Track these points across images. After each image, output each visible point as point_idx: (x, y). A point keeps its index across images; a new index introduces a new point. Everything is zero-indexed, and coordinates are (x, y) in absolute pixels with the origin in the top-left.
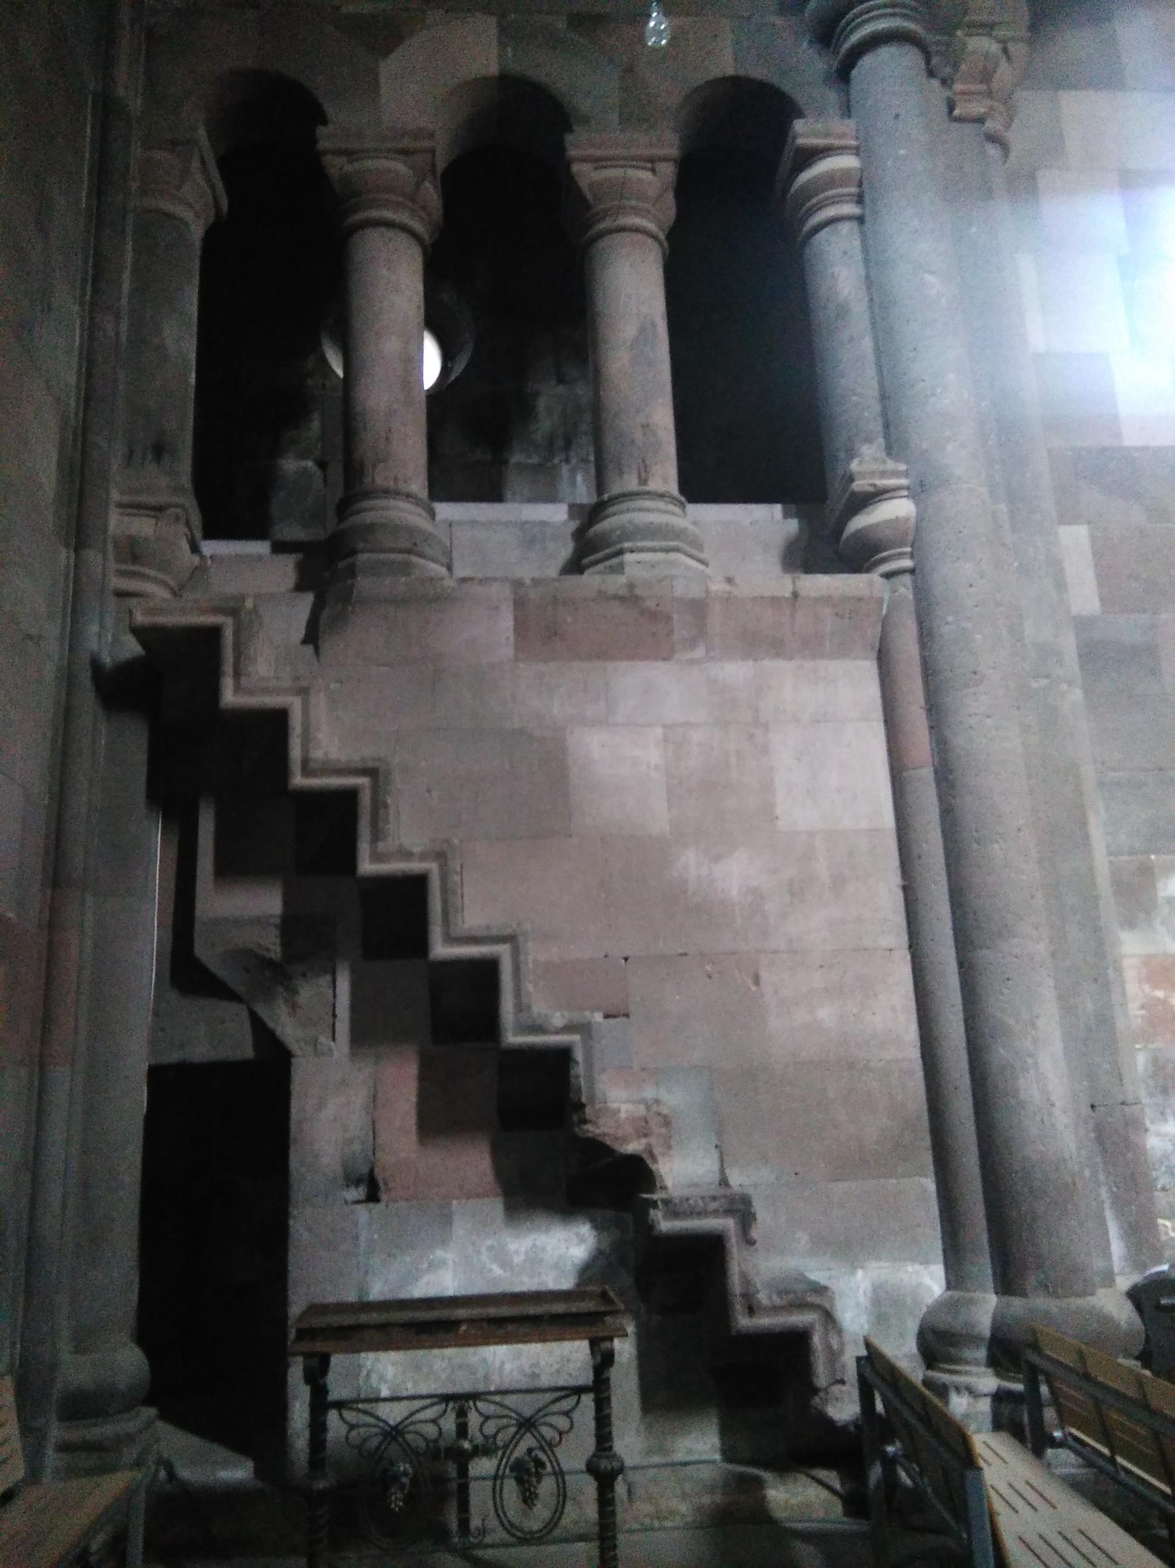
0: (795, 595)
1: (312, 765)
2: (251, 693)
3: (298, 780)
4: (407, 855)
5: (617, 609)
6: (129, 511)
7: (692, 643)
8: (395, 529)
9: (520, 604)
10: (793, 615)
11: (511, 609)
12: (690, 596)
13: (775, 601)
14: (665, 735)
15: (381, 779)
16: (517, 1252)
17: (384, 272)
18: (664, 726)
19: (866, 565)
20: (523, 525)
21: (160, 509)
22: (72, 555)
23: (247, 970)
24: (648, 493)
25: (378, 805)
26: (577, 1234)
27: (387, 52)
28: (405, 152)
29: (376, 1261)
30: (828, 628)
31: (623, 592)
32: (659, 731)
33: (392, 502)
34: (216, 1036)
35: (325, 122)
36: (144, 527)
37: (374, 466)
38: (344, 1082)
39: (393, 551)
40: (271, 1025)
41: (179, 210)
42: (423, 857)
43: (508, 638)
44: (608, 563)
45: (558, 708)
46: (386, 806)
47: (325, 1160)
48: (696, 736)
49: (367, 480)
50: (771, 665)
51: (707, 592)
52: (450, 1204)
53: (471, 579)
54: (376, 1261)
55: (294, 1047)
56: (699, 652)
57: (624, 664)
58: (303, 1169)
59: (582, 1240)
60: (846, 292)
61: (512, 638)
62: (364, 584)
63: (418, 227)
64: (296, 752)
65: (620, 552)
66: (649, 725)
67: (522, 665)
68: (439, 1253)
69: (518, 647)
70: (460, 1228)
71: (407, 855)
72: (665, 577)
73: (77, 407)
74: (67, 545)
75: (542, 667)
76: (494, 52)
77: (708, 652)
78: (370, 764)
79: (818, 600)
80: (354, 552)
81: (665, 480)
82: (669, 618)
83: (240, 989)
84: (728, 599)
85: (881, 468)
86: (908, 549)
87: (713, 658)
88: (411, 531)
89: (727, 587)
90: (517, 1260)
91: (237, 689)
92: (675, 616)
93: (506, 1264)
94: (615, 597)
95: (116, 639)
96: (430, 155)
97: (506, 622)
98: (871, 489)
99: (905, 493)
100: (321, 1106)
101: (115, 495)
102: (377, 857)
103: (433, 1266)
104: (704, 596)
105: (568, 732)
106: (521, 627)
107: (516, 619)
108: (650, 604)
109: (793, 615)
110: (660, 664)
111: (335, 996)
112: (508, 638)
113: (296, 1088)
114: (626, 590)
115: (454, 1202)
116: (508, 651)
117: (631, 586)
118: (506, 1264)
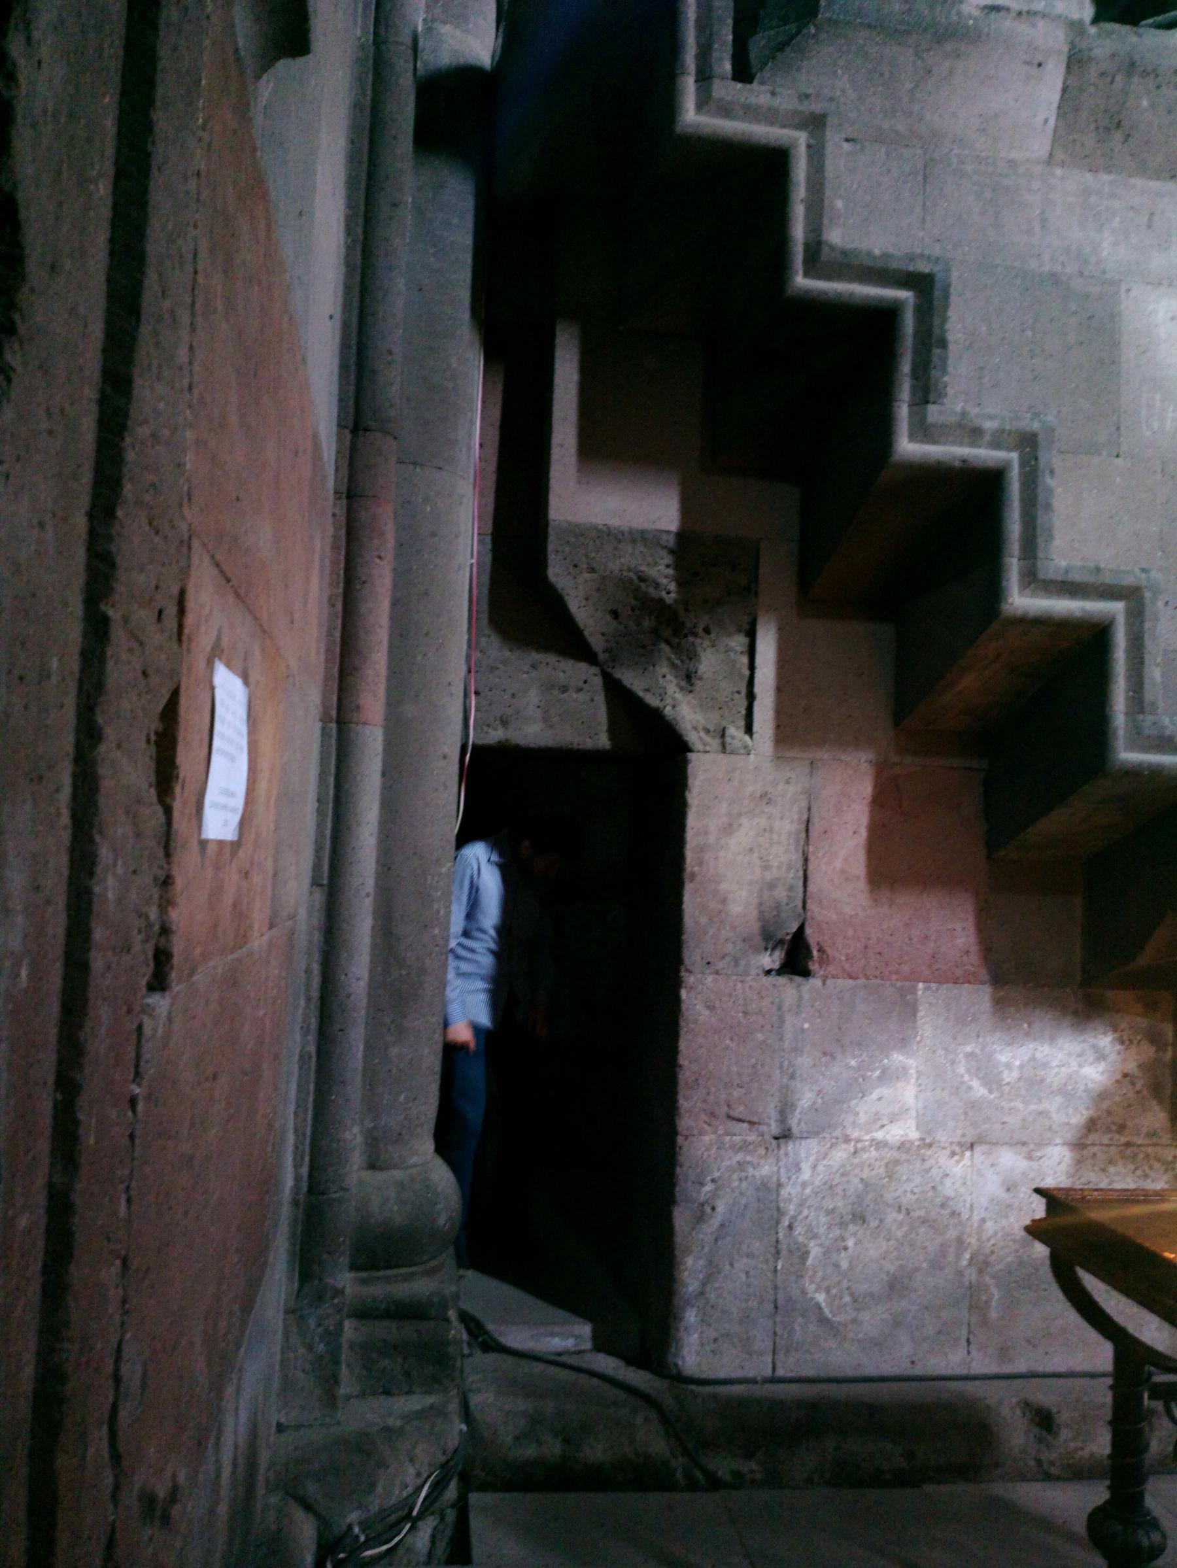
3: (801, 281)
4: (975, 434)
11: (1062, 69)
15: (937, 293)
16: (1008, 1066)
23: (615, 614)
25: (931, 341)
26: (1094, 1046)
29: (804, 1062)
34: (553, 708)
38: (765, 798)
40: (652, 700)
42: (995, 444)
43: (1046, 121)
45: (1111, 250)
46: (943, 344)
47: (735, 909)
52: (914, 991)
53: (1008, 9)
54: (804, 1062)
55: (693, 738)
58: (703, 920)
59: (1101, 1057)
64: (798, 231)
67: (1059, 172)
68: (898, 1057)
69: (1055, 140)
70: (927, 1026)
71: (975, 434)
78: (924, 267)
83: (596, 642)
90: (1009, 1077)
91: (700, 106)
93: (992, 1081)
100: (728, 829)
102: (923, 431)
103: (888, 1077)
105: (1123, 288)
107: (1065, 89)
111: (752, 667)
112: (1046, 121)
113: (694, 797)
115: (921, 985)
116: (1040, 146)
118: (992, 1081)
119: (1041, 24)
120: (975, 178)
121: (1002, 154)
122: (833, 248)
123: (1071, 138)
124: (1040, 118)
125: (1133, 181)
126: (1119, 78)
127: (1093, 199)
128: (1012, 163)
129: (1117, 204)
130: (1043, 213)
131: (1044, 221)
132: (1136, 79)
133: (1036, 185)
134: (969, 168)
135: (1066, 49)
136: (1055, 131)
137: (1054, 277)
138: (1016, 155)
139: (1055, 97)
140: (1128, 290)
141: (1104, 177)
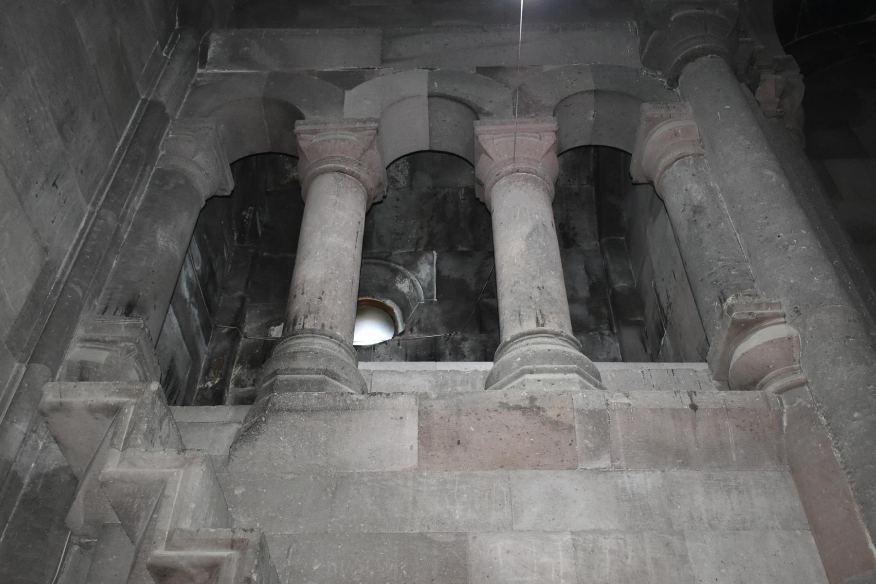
0: (694, 407)
1: (175, 537)
2: (133, 464)
5: (517, 419)
6: (87, 345)
7: (595, 453)
8: (317, 355)
9: (423, 414)
10: (694, 427)
11: (416, 418)
12: (591, 408)
13: (675, 413)
14: (574, 540)
17: (334, 197)
18: (572, 533)
19: (758, 385)
20: (436, 373)
21: (114, 342)
22: (24, 369)
24: (545, 332)
27: (350, 88)
28: (354, 130)
30: (731, 440)
31: (526, 403)
32: (568, 537)
33: (317, 341)
35: (301, 117)
36: (101, 356)
37: (306, 317)
39: (309, 371)
41: (191, 169)
43: (412, 447)
44: (509, 386)
45: (459, 513)
48: (608, 544)
49: (298, 327)
50: (677, 473)
51: (608, 404)
53: (381, 394)
56: (604, 462)
57: (528, 473)
60: (699, 198)
61: (416, 447)
62: (281, 398)
63: (363, 175)
64: (165, 524)
65: (523, 373)
66: (555, 532)
69: (419, 457)
72: (564, 392)
73: (67, 266)
74: (21, 361)
75: (446, 475)
76: (426, 85)
77: (612, 462)
79: (715, 412)
80: (275, 373)
81: (561, 326)
82: (571, 428)
84: (627, 410)
85: (756, 301)
86: (798, 365)
87: (619, 469)
88: (330, 358)
89: (626, 401)
92: (577, 426)
94: (517, 408)
95: (45, 447)
96: (375, 132)
97: (411, 431)
98: (750, 318)
99: (783, 320)
101: (80, 332)
104: (605, 407)
105: (470, 537)
106: (425, 436)
107: (420, 428)
108: (552, 414)
109: (694, 427)
110: (565, 473)
112: (412, 447)
114: (527, 402)
116: (411, 460)
117: (532, 399)
119: (401, 398)
120: (369, 484)
121: (388, 469)
122: (182, 530)
123: (430, 454)
124: (408, 446)
125: (475, 472)
126: (452, 418)
127: (448, 487)
128: (394, 474)
129: (464, 487)
130: (414, 498)
131: (415, 502)
132: (463, 417)
133: (410, 483)
134: (366, 479)
135: (416, 408)
136: (419, 453)
137: (422, 536)
138: (397, 468)
139: (415, 432)
140: (475, 537)
141: (458, 473)
